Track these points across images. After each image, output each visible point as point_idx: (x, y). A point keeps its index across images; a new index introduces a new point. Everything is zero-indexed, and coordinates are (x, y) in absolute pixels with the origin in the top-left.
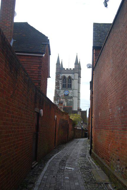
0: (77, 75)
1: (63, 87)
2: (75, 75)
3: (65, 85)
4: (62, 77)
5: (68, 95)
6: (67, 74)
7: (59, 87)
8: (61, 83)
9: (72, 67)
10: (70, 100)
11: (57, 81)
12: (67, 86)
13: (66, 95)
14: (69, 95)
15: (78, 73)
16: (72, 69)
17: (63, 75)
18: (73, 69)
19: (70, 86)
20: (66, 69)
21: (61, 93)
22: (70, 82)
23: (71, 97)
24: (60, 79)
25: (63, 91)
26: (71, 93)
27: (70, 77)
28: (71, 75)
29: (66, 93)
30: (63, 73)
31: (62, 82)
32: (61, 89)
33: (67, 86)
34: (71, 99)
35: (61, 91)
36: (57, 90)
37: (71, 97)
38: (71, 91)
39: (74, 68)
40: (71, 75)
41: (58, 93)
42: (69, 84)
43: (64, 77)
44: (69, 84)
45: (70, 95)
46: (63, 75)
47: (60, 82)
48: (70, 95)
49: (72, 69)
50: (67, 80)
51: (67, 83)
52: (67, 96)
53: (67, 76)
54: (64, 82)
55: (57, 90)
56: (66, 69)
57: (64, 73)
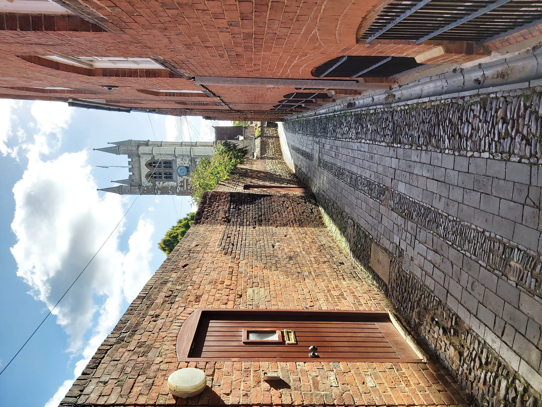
0: (142, 149)
2: (144, 154)
5: (186, 167)
6: (142, 170)
9: (124, 159)
11: (157, 192)
12: (167, 170)
13: (188, 171)
14: (188, 165)
15: (138, 146)
16: (130, 160)
17: (144, 179)
18: (129, 157)
19: (168, 164)
20: (131, 174)
23: (193, 160)
24: (155, 185)
30: (141, 180)
33: (167, 170)
36: (178, 191)
37: (193, 160)
38: (179, 161)
39: (127, 155)
42: (163, 165)
44: (163, 165)
46: (144, 179)
47: (160, 184)
48: (187, 163)
49: (130, 160)
50: (156, 170)
51: (162, 170)
53: (145, 171)
54: (160, 178)
55: (178, 191)
56: (131, 174)
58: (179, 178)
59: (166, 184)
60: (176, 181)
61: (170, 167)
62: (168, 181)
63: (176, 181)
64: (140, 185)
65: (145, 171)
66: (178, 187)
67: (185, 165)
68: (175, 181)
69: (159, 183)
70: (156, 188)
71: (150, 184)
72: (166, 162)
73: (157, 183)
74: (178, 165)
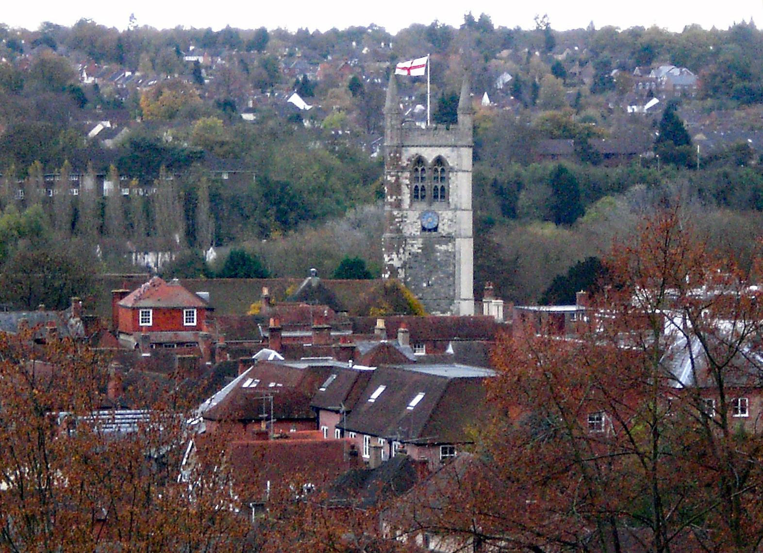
3: (423, 189)
4: (409, 160)
5: (436, 229)
10: (443, 248)
13: (430, 230)
14: (440, 230)
17: (413, 151)
27: (439, 161)
28: (444, 152)
31: (410, 179)
32: (408, 207)
34: (447, 244)
35: (410, 213)
40: (444, 152)
43: (420, 160)
45: (444, 229)
46: (413, 151)
48: (444, 229)
58: (417, 214)
67: (440, 225)
68: (411, 205)
69: (406, 178)
74: (440, 212)
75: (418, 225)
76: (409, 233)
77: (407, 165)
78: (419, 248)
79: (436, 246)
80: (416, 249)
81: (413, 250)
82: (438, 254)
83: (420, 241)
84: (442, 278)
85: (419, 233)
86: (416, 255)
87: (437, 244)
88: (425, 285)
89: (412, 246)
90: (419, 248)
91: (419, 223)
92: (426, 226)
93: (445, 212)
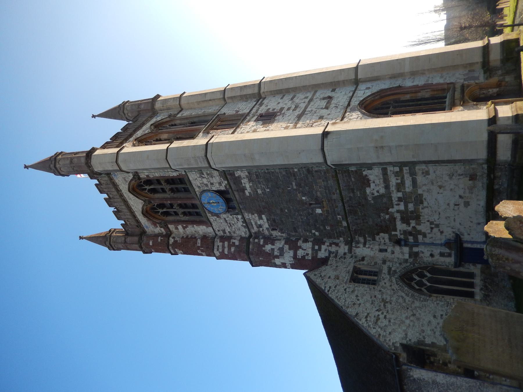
1: (198, 214)
5: (220, 193)
7: (204, 238)
8: (180, 227)
10: (247, 184)
13: (228, 201)
14: (222, 188)
17: (143, 221)
19: (179, 184)
21: (228, 230)
22: (158, 181)
25: (212, 219)
26: (205, 181)
28: (124, 188)
29: (212, 203)
30: (138, 221)
32: (210, 230)
38: (196, 181)
41: (229, 249)
46: (143, 221)
48: (218, 183)
49: (96, 181)
52: (231, 196)
57: (134, 216)
59: (191, 230)
60: (209, 224)
61: (186, 190)
62: (193, 223)
63: (209, 224)
64: (143, 233)
65: (137, 205)
66: (218, 243)
67: (214, 189)
69: (177, 228)
70: (171, 241)
71: (158, 230)
72: (170, 181)
73: (171, 227)
74: (197, 189)
75: (228, 217)
76: (244, 229)
77: (161, 227)
78: (261, 218)
79: (248, 194)
80: (264, 222)
81: (266, 226)
82: (260, 192)
83: (247, 216)
84: (299, 185)
85: (240, 217)
86: (274, 225)
87: (244, 192)
88: (319, 211)
89: (260, 226)
90: (261, 218)
91: (224, 216)
92: (224, 207)
93: (193, 182)
